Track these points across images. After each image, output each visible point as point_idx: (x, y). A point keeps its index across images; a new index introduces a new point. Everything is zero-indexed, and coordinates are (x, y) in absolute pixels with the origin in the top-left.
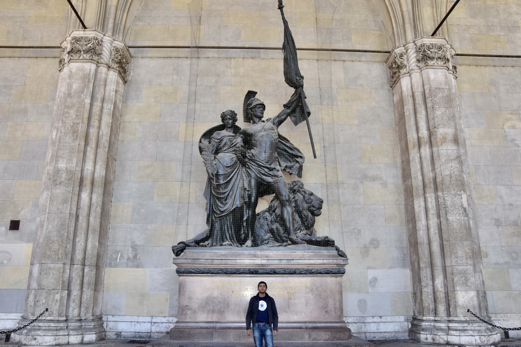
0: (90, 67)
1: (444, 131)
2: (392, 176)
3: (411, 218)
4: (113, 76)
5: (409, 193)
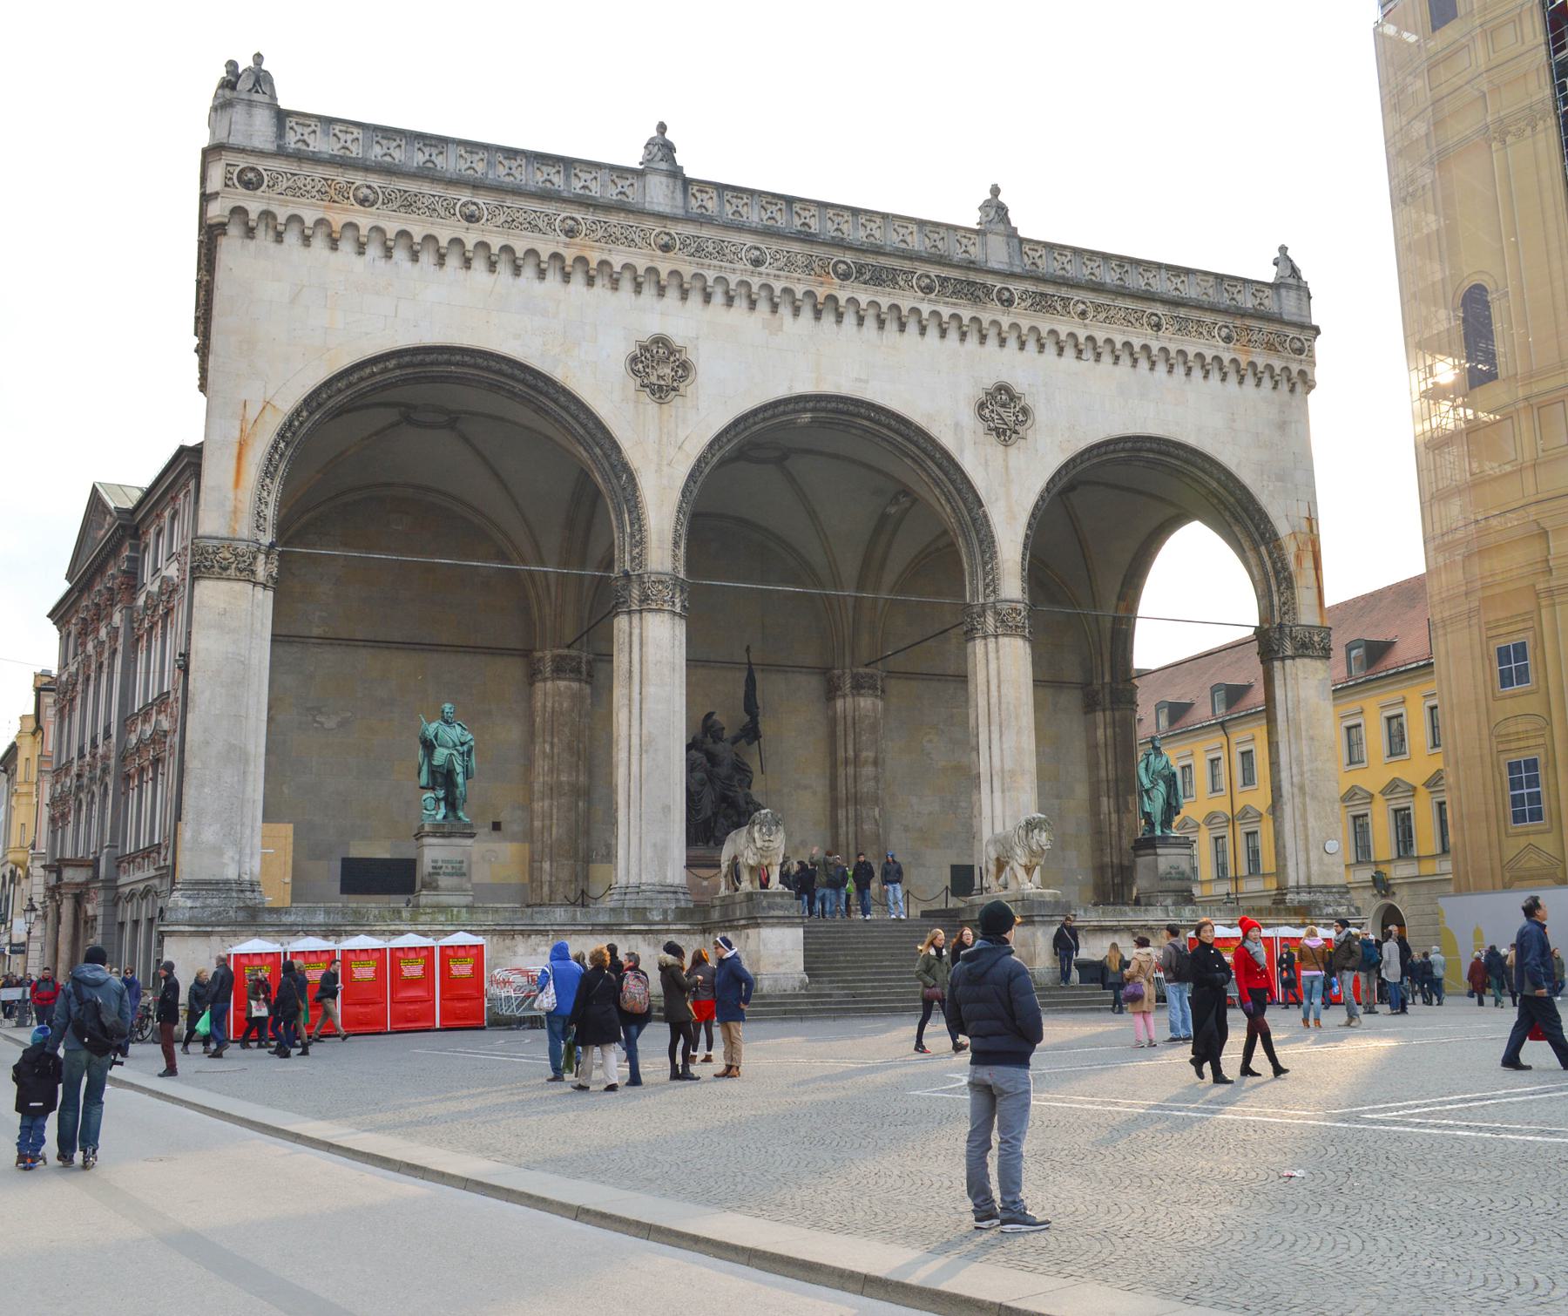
0: (575, 685)
1: (868, 754)
2: (821, 786)
3: (834, 825)
4: (587, 689)
5: (834, 803)
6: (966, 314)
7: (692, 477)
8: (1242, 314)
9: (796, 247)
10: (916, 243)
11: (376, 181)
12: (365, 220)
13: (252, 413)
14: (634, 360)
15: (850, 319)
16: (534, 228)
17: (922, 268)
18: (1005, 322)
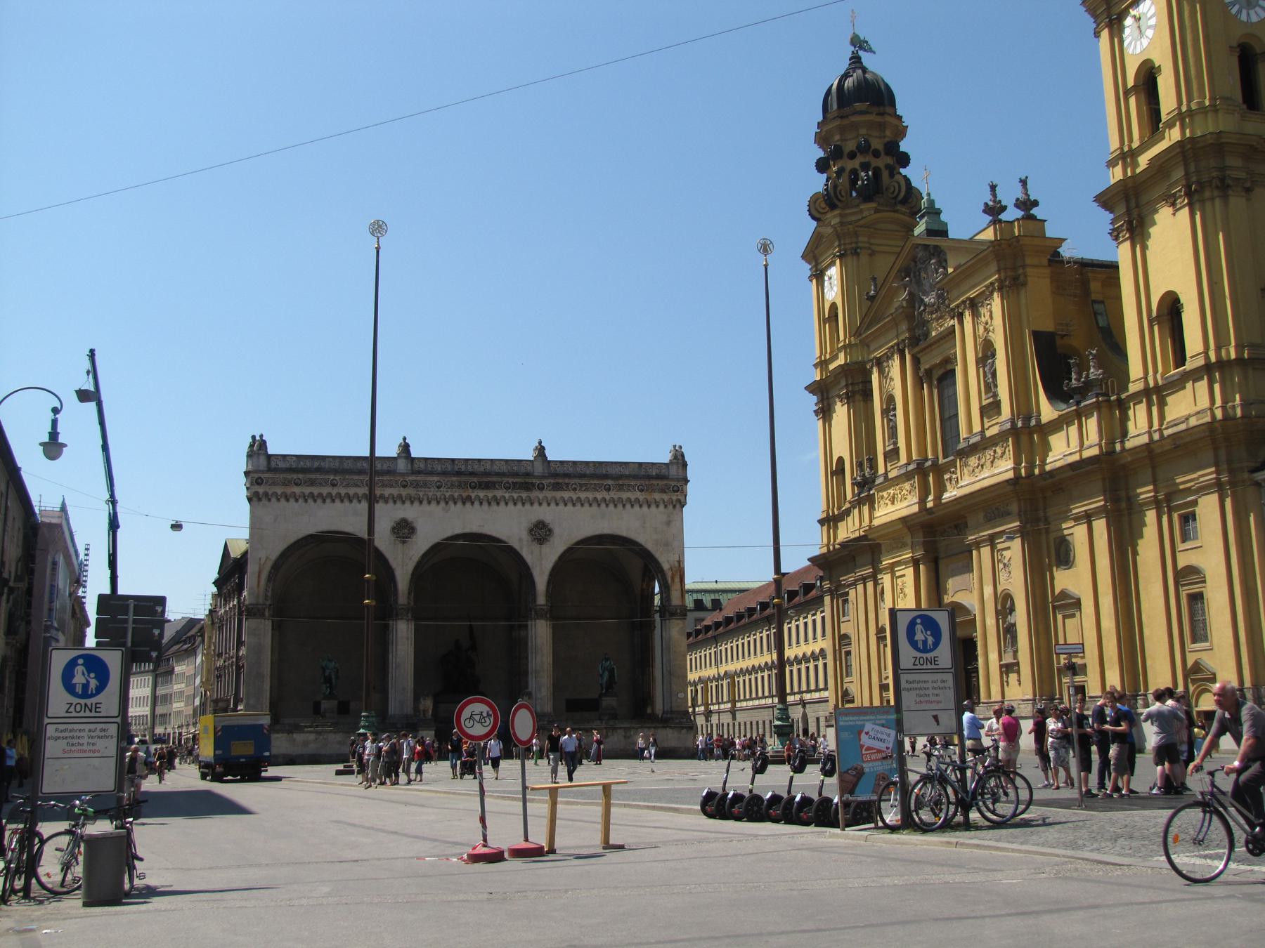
6: (524, 495)
7: (416, 568)
8: (650, 477)
9: (454, 479)
10: (504, 469)
11: (301, 476)
12: (297, 490)
13: (263, 560)
14: (394, 528)
15: (477, 503)
16: (357, 486)
17: (505, 480)
18: (541, 496)
